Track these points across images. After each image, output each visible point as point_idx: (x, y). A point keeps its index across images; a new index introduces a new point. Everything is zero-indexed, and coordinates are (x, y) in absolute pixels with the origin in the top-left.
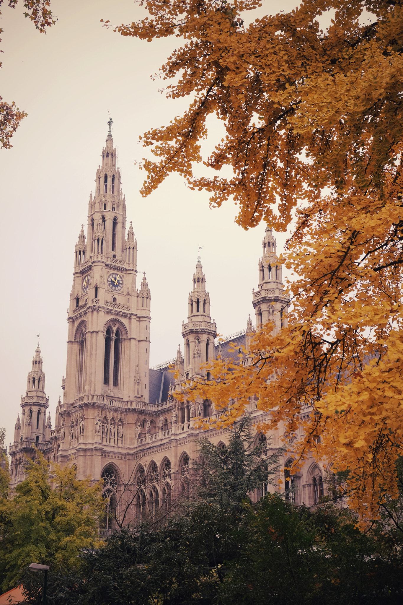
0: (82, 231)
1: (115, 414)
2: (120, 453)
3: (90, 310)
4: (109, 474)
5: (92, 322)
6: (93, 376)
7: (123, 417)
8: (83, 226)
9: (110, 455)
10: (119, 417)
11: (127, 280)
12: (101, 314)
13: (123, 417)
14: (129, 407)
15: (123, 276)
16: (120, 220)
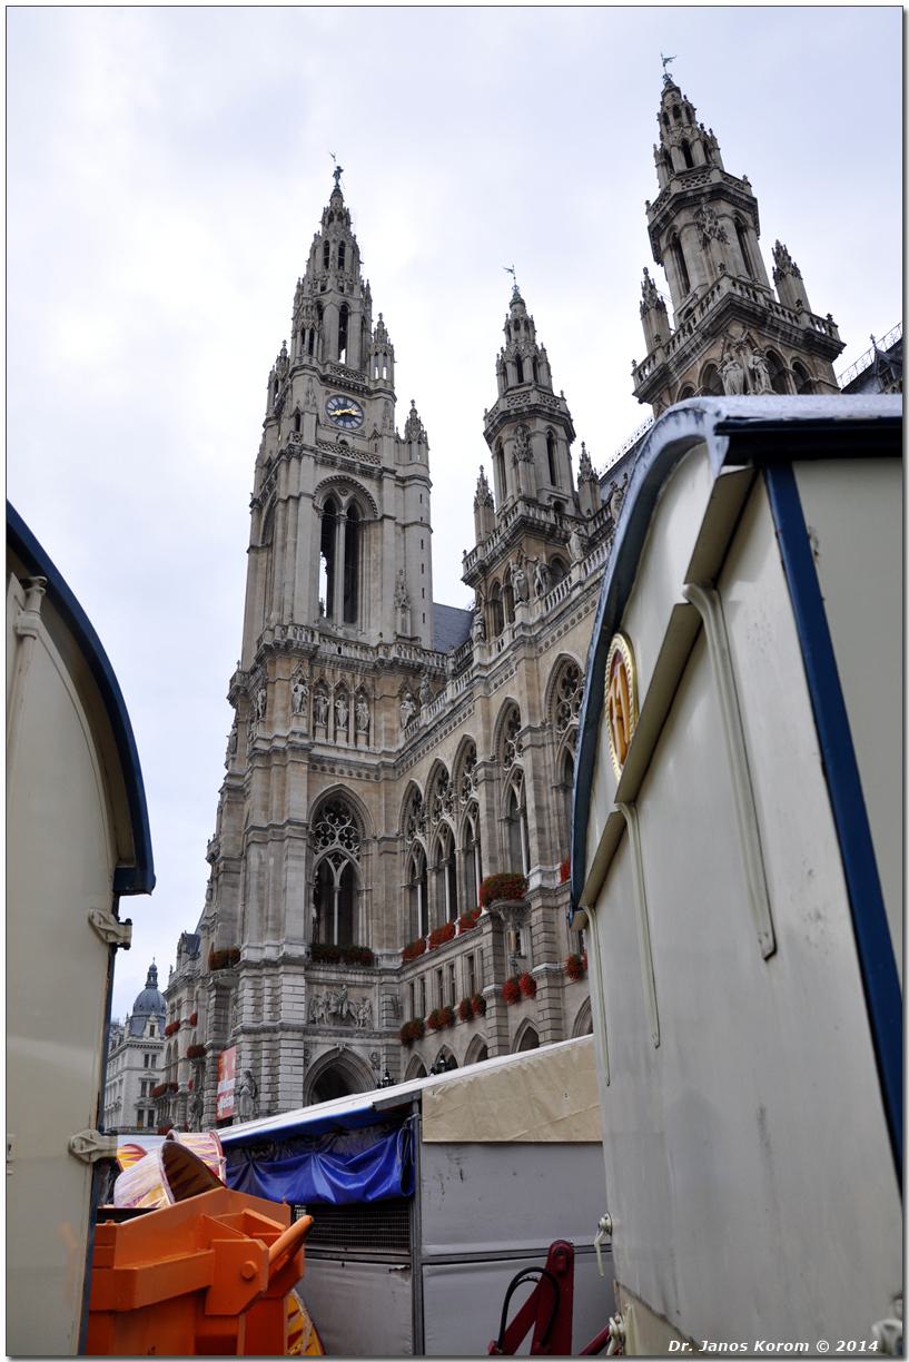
0: (284, 350)
1: (348, 676)
2: (363, 765)
3: (283, 457)
4: (337, 815)
5: (287, 481)
6: (288, 588)
8: (285, 342)
9: (337, 768)
10: (358, 682)
11: (374, 410)
12: (308, 461)
13: (369, 682)
14: (382, 657)
15: (364, 404)
16: (355, 306)
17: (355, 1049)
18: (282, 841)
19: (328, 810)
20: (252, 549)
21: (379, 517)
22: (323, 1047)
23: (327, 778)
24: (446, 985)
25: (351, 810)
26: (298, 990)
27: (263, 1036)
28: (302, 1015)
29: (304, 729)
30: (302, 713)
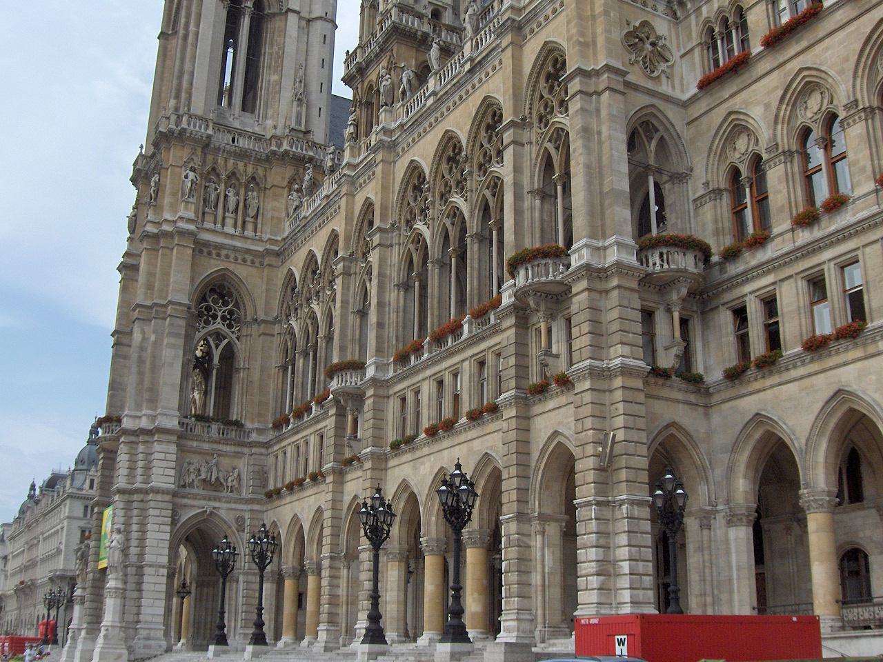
1: (241, 165)
2: (248, 251)
6: (186, 77)
7: (261, 172)
9: (224, 252)
10: (250, 170)
13: (261, 172)
14: (274, 148)
17: (223, 513)
18: (165, 319)
19: (213, 291)
20: (163, 36)
21: (283, 11)
22: (193, 509)
23: (212, 261)
24: (302, 459)
25: (235, 293)
26: (170, 457)
27: (135, 497)
28: (172, 480)
29: (191, 215)
30: (191, 200)
